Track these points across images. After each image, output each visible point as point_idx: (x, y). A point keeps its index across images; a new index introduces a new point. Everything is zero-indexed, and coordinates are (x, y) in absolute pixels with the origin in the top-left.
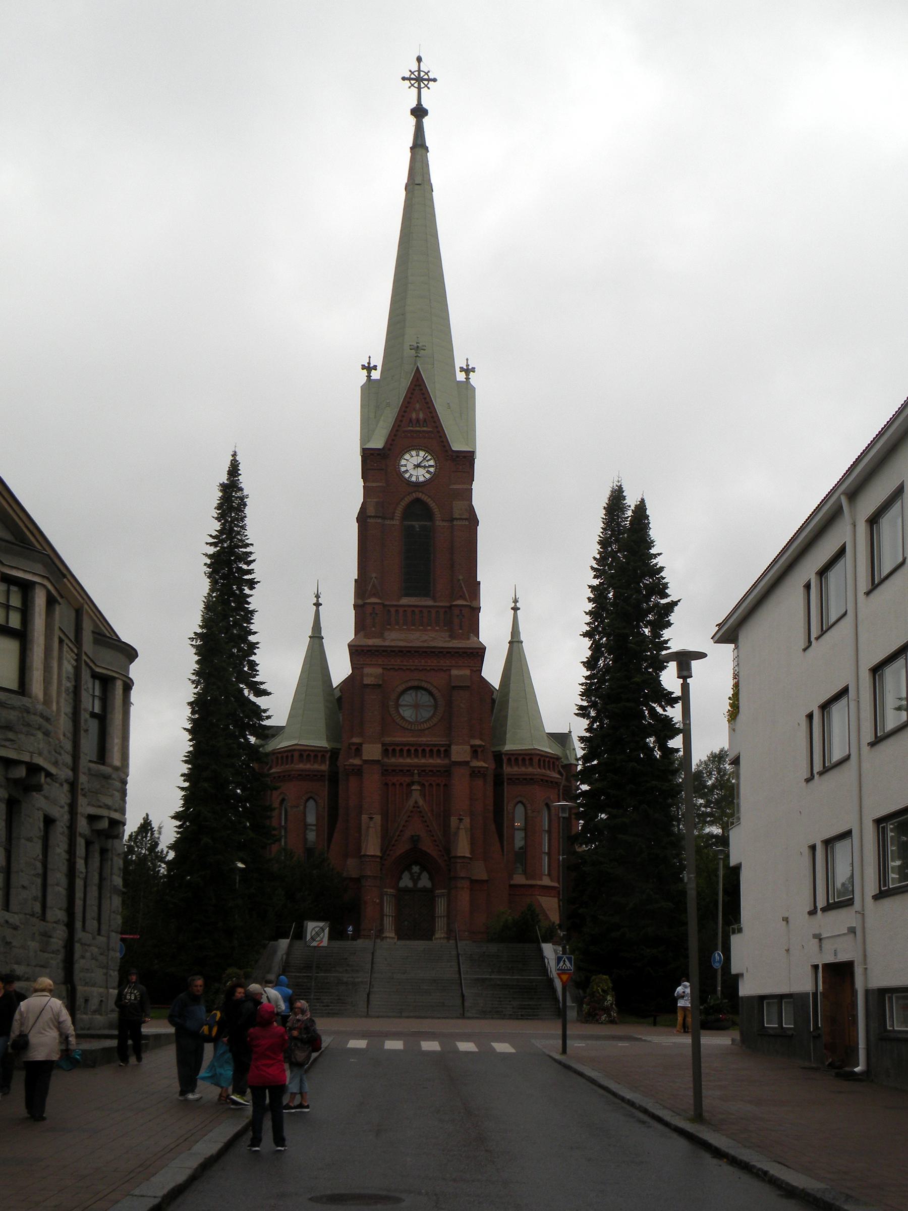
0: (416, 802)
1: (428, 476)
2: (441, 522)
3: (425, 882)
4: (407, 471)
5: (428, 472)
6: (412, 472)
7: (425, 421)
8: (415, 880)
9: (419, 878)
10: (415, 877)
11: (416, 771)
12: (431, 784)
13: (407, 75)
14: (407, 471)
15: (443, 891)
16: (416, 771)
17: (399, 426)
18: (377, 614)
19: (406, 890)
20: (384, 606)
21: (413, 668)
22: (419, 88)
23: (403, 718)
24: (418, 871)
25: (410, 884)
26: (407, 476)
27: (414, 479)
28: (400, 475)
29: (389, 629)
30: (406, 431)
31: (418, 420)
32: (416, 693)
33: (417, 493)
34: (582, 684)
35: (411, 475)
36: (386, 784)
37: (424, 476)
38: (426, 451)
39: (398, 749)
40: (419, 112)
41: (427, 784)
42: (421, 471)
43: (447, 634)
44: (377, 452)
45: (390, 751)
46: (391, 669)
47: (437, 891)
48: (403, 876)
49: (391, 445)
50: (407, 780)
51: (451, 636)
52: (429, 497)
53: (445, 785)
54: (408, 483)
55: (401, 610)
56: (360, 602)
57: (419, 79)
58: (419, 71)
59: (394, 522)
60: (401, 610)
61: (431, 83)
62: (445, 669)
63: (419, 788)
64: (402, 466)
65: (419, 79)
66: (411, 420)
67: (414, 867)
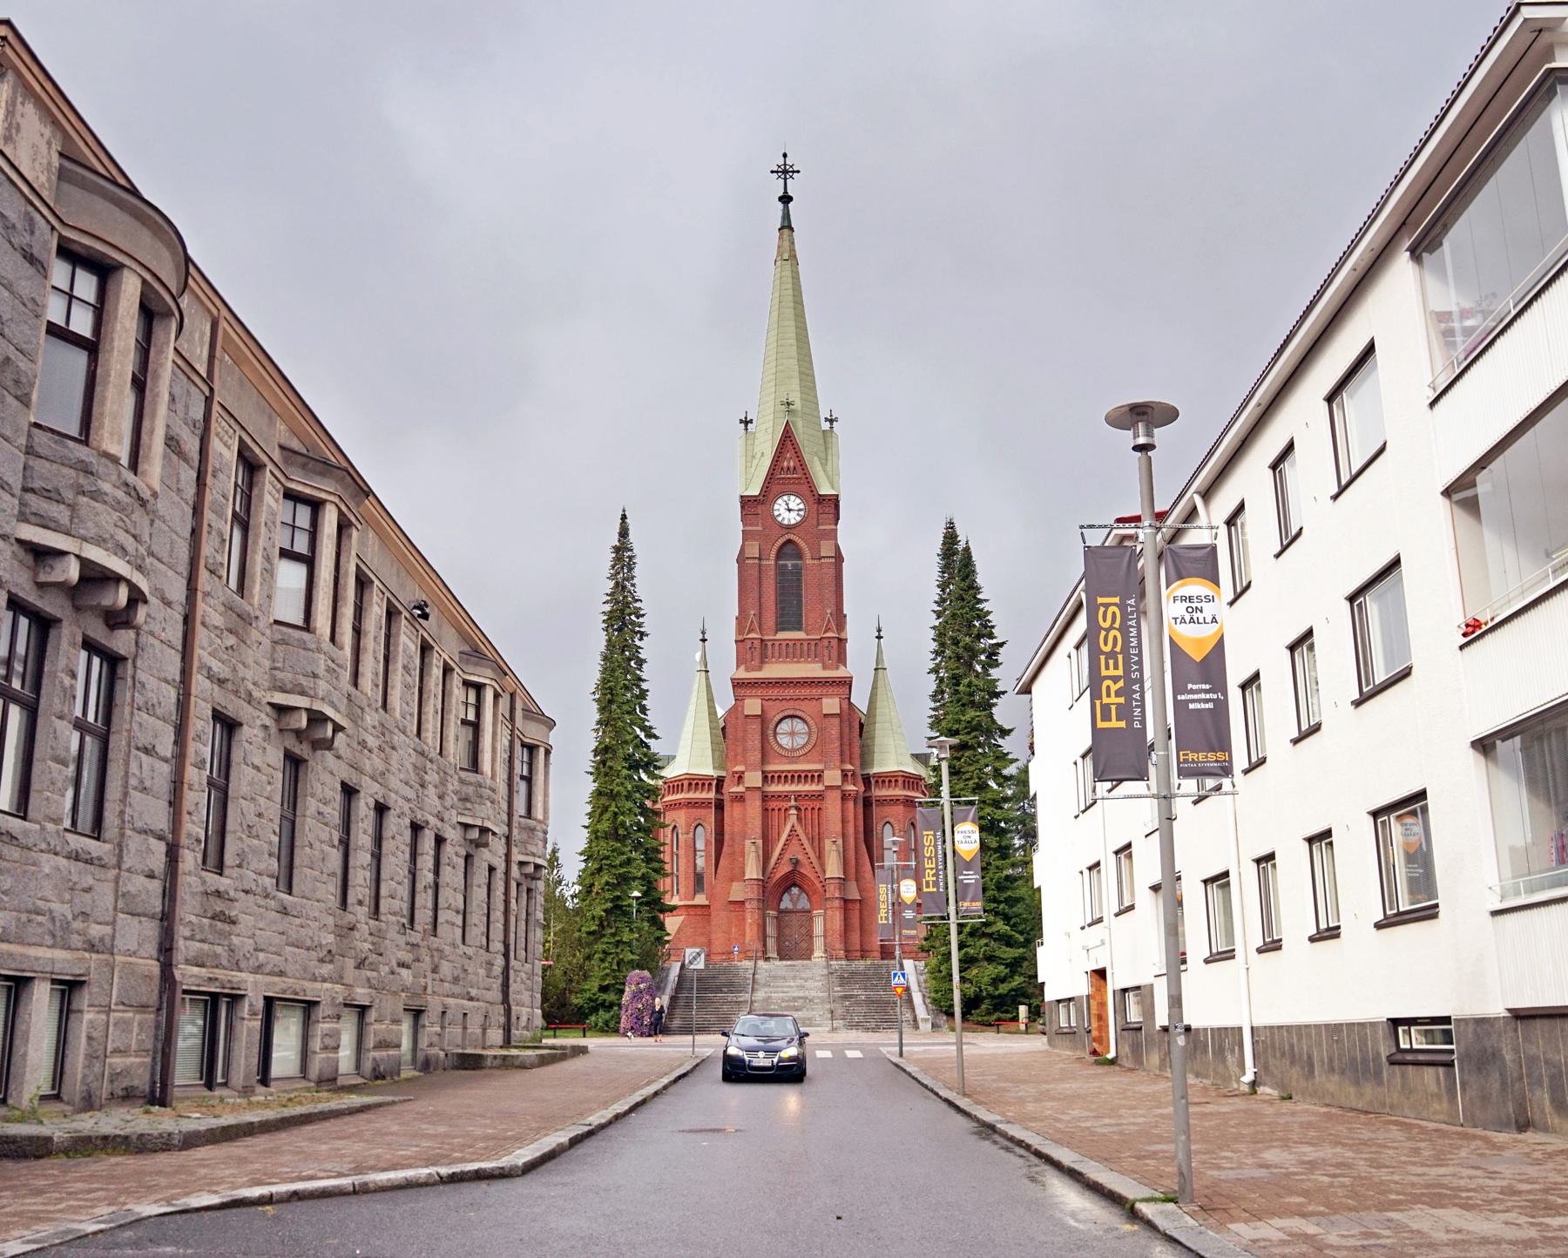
1: (799, 519)
3: (804, 903)
6: (783, 515)
9: (798, 899)
13: (775, 169)
19: (787, 911)
20: (762, 640)
22: (785, 179)
23: (780, 746)
25: (790, 906)
26: (780, 519)
27: (786, 522)
28: (774, 518)
34: (931, 717)
35: (783, 519)
36: (767, 809)
39: (776, 775)
40: (786, 199)
41: (803, 808)
43: (820, 665)
51: (825, 668)
54: (781, 525)
56: (741, 638)
57: (785, 172)
58: (785, 165)
61: (795, 174)
65: (785, 172)
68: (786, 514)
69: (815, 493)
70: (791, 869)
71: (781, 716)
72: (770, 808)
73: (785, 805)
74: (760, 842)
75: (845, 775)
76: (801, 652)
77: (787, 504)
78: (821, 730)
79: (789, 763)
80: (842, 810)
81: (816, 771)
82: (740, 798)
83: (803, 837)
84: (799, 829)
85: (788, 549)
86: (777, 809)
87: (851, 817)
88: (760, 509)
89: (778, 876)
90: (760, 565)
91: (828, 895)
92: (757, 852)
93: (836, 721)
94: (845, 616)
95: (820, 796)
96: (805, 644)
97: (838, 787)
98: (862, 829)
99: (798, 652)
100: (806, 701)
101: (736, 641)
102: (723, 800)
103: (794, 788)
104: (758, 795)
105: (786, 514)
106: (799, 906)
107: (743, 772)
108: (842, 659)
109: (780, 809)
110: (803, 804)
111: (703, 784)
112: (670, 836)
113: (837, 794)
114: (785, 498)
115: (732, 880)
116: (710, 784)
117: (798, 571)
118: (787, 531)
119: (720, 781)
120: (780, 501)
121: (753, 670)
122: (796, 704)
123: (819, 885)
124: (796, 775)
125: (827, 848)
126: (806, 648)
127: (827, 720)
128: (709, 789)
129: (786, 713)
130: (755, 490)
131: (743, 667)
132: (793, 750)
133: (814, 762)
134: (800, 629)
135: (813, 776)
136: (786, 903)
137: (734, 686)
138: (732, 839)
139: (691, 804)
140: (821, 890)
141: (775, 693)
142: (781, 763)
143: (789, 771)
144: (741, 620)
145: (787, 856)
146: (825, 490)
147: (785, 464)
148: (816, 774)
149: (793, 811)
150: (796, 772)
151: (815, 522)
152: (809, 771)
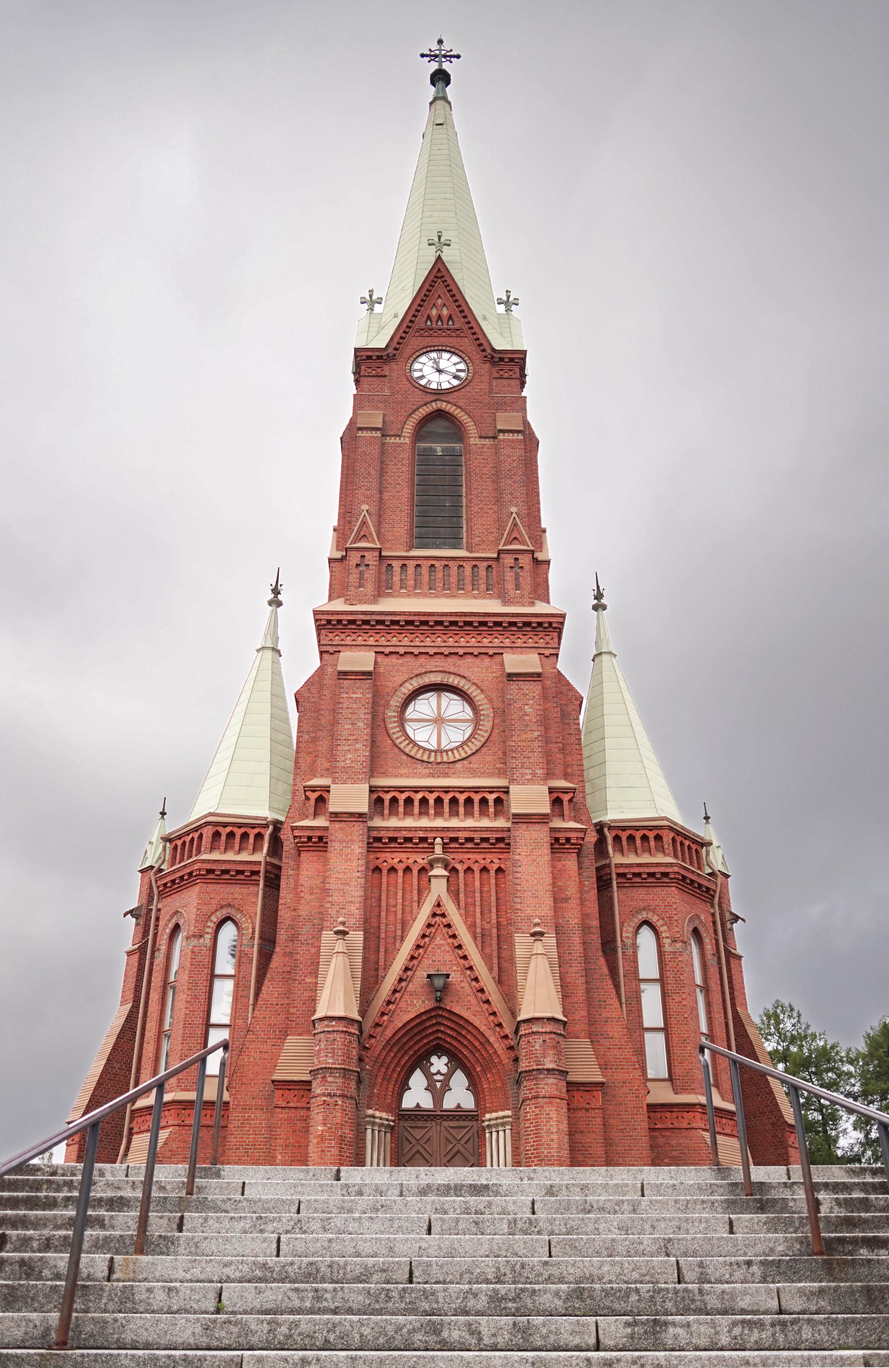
0: (439, 905)
2: (477, 440)
4: (422, 377)
7: (450, 317)
8: (438, 1091)
9: (446, 1087)
10: (438, 1085)
11: (438, 840)
14: (422, 377)
15: (501, 1114)
16: (438, 840)
19: (418, 1115)
24: (444, 1070)
25: (427, 1102)
26: (423, 382)
27: (434, 386)
31: (440, 317)
32: (439, 698)
33: (439, 403)
36: (377, 869)
38: (454, 353)
39: (402, 797)
40: (441, 78)
45: (387, 803)
46: (391, 653)
47: (488, 1116)
48: (411, 1082)
50: (422, 860)
52: (459, 407)
53: (499, 870)
54: (425, 389)
55: (411, 564)
56: (339, 555)
60: (411, 564)
62: (491, 652)
63: (446, 873)
66: (429, 317)
67: (434, 1059)
70: (429, 1004)
71: (416, 684)
72: (385, 867)
74: (357, 937)
75: (556, 802)
77: (436, 362)
78: (502, 713)
79: (431, 775)
83: (465, 937)
84: (450, 907)
85: (438, 426)
86: (400, 867)
87: (572, 890)
88: (386, 370)
90: (383, 444)
91: (523, 1065)
92: (348, 953)
96: (468, 567)
97: (543, 819)
98: (595, 923)
99: (454, 580)
100: (469, 660)
101: (331, 560)
102: (279, 868)
103: (439, 823)
104: (357, 831)
106: (449, 1103)
107: (327, 789)
108: (541, 591)
109: (408, 869)
110: (461, 859)
111: (245, 836)
112: (163, 948)
113: (539, 835)
114: (434, 355)
115: (284, 1034)
116: (259, 837)
117: (454, 460)
118: (436, 397)
119: (277, 825)
120: (423, 359)
122: (449, 664)
123: (499, 1046)
124: (447, 798)
125: (520, 951)
127: (514, 686)
130: (381, 342)
132: (439, 751)
133: (483, 775)
134: (455, 547)
135: (484, 801)
137: (319, 628)
138: (293, 938)
140: (505, 1057)
141: (406, 641)
142: (415, 775)
143: (431, 789)
144: (341, 532)
145: (421, 975)
146: (499, 343)
147: (434, 312)
148: (491, 797)
149: (439, 871)
150: (447, 790)
151: (484, 386)
152: (476, 790)
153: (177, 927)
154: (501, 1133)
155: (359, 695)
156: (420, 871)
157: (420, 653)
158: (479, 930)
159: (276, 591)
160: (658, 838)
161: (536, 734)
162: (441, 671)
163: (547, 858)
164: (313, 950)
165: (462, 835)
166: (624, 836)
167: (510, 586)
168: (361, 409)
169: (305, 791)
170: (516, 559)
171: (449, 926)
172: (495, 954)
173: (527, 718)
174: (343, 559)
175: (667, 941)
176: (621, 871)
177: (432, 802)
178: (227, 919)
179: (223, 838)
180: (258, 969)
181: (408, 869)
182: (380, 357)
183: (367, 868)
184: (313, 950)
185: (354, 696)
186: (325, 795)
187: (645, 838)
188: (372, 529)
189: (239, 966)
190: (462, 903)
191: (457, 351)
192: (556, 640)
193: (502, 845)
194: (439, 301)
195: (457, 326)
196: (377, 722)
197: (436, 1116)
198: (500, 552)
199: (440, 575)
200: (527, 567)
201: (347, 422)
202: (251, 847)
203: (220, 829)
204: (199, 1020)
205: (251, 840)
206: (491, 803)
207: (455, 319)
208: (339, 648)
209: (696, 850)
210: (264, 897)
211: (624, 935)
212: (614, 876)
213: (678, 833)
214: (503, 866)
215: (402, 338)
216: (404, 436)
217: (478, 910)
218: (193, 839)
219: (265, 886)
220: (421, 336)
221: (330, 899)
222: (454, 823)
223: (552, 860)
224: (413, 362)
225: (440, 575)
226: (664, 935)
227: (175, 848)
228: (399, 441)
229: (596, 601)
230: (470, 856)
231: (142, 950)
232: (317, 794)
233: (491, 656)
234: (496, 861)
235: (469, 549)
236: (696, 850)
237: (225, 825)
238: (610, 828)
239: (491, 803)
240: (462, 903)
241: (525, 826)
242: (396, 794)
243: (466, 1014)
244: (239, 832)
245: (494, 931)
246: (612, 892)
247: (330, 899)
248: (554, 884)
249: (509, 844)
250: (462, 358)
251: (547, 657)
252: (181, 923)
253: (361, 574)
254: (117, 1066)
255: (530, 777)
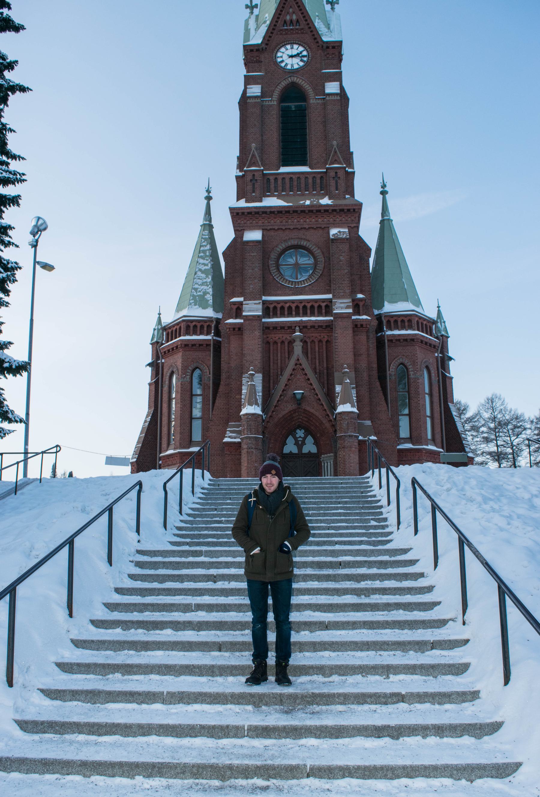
0: (298, 360)
1: (302, 64)
2: (314, 100)
3: (310, 447)
4: (282, 61)
5: (301, 61)
7: (297, 21)
8: (300, 445)
9: (304, 443)
10: (300, 442)
12: (313, 341)
14: (282, 61)
17: (275, 25)
18: (256, 180)
21: (292, 227)
24: (303, 436)
25: (295, 450)
26: (283, 65)
27: (289, 67)
28: (277, 64)
29: (269, 196)
30: (281, 30)
31: (291, 21)
33: (292, 78)
35: (286, 65)
36: (268, 343)
37: (298, 64)
38: (300, 45)
42: (296, 60)
44: (256, 48)
45: (271, 309)
46: (271, 229)
47: (323, 456)
49: (268, 40)
53: (327, 341)
54: (284, 69)
56: (241, 174)
59: (272, 103)
64: (278, 57)
66: (285, 22)
68: (289, 61)
69: (319, 40)
70: (294, 406)
71: (283, 246)
73: (286, 337)
76: (306, 185)
80: (354, 344)
81: (323, 300)
82: (238, 330)
86: (279, 342)
89: (280, 416)
93: (345, 247)
94: (352, 153)
95: (329, 327)
97: (349, 315)
98: (375, 366)
99: (303, 185)
100: (312, 231)
101: (237, 177)
103: (298, 319)
105: (289, 61)
106: (305, 450)
107: (241, 303)
111: (202, 327)
112: (167, 382)
116: (209, 327)
119: (218, 321)
121: (254, 201)
123: (328, 425)
124: (301, 306)
126: (310, 181)
128: (208, 334)
129: (290, 243)
131: (244, 200)
136: (290, 447)
137: (233, 217)
138: (229, 377)
139: (186, 345)
140: (331, 430)
147: (288, 18)
150: (301, 301)
153: (172, 373)
154: (329, 463)
155: (255, 254)
156: (288, 343)
157: (286, 229)
158: (318, 371)
159: (208, 191)
160: (410, 321)
161: (347, 271)
162: (297, 238)
163: (351, 335)
164: (239, 383)
165: (309, 325)
166: (392, 320)
167: (333, 188)
168: (249, 85)
169: (230, 305)
170: (336, 173)
171: (303, 369)
172: (326, 382)
173: (341, 263)
174: (243, 176)
175: (412, 373)
176: (390, 338)
177: (294, 308)
178: (197, 368)
179: (192, 328)
180: (213, 392)
181: (283, 342)
182: (258, 50)
183: (263, 342)
184: (239, 383)
185: (253, 254)
186: (240, 307)
187: (403, 321)
188: (258, 158)
189: (204, 390)
190: (310, 358)
191: (302, 43)
192: (357, 218)
193: (329, 329)
194: (291, 10)
195: (302, 27)
196: (265, 268)
197: (300, 455)
198: (327, 169)
199: (295, 183)
200: (342, 177)
201: (241, 93)
202: (205, 332)
203: (189, 324)
204: (187, 416)
205: (205, 329)
206: (323, 308)
207: (301, 22)
208: (244, 228)
209: (430, 326)
210: (214, 357)
211: (391, 370)
212: (386, 341)
213: (420, 318)
214: (329, 339)
215: (270, 37)
216: (274, 100)
217: (317, 361)
218: (176, 329)
219: (214, 351)
220: (281, 34)
221: (245, 358)
222: (305, 319)
223: (354, 336)
224: (277, 52)
225: (295, 183)
226: (410, 370)
227: (168, 335)
228: (271, 104)
229: (382, 189)
230: (313, 335)
231: (156, 383)
232: (236, 306)
233: (323, 229)
234: (326, 337)
235: (311, 168)
236: (430, 326)
237: (192, 321)
238: (385, 316)
239: (323, 308)
240: (310, 358)
241: (340, 320)
242: (276, 304)
243: (312, 411)
244: (199, 325)
245: (325, 371)
246: (384, 349)
247: (245, 358)
248: (354, 348)
249: (332, 328)
250: (305, 48)
251: (352, 228)
252: (175, 370)
253: (254, 185)
254: (150, 437)
255: (342, 294)
